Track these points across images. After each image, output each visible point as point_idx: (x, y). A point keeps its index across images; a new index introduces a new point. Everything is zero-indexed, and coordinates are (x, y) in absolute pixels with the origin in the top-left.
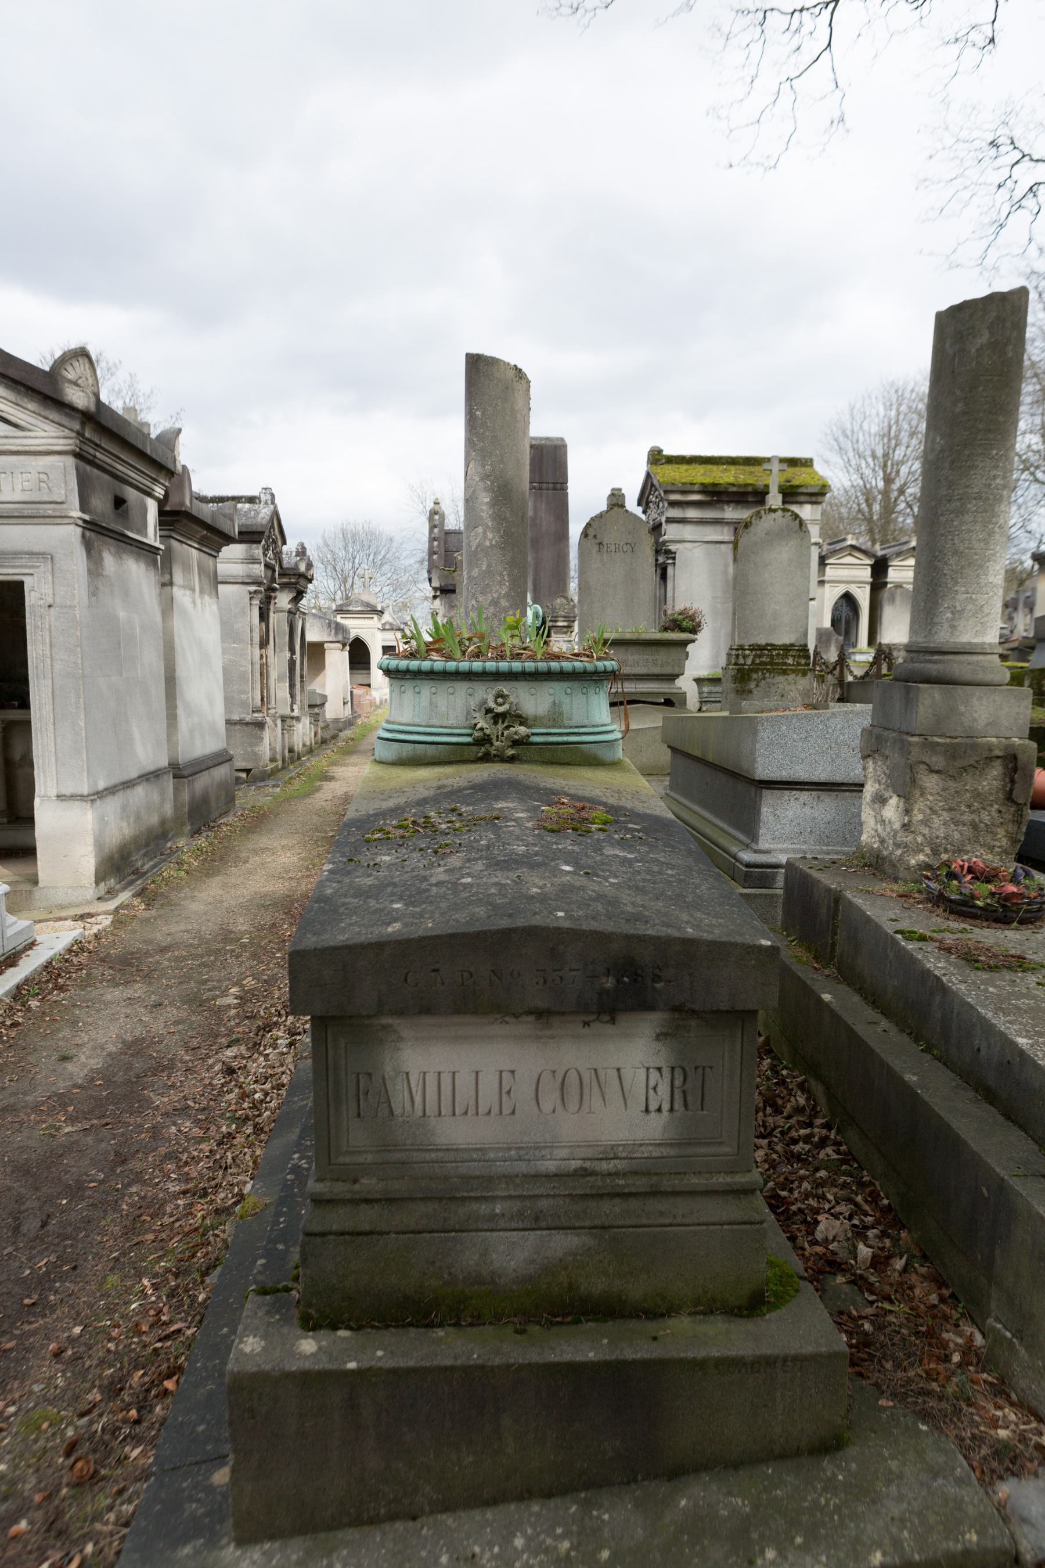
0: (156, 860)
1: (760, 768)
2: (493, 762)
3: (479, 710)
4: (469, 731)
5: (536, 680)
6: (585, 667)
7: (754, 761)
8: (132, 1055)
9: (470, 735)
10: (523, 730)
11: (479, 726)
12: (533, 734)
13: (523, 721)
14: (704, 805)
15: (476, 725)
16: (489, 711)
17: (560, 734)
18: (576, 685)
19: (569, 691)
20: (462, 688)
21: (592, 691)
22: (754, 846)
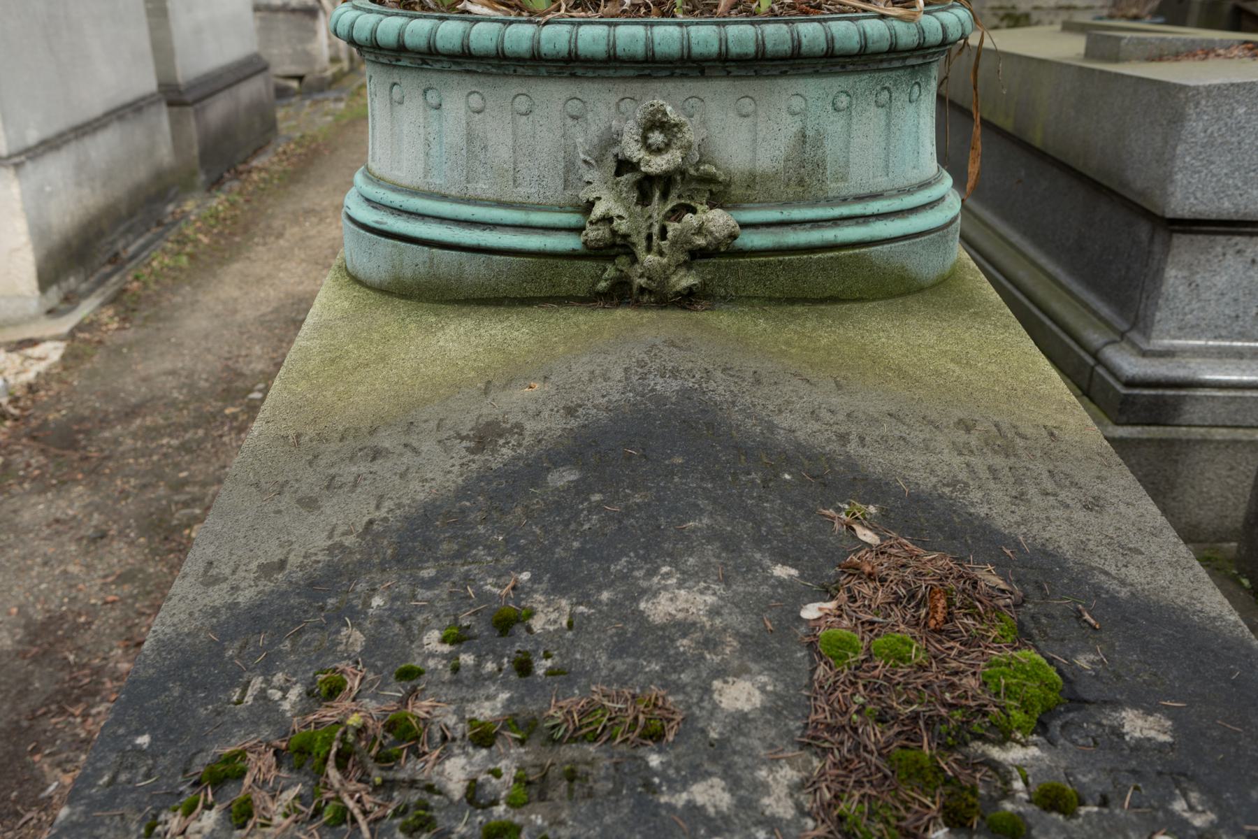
0: (148, 236)
1: (1179, 195)
2: (638, 305)
3: (599, 161)
4: (572, 219)
5: (758, 75)
6: (894, 36)
7: (1168, 178)
8: (35, 660)
9: (578, 230)
10: (718, 220)
11: (598, 211)
12: (744, 226)
13: (718, 192)
14: (1007, 217)
15: (590, 205)
16: (624, 166)
17: (816, 223)
18: (860, 82)
19: (843, 101)
20: (553, 96)
21: (901, 97)
22: (1135, 336)
